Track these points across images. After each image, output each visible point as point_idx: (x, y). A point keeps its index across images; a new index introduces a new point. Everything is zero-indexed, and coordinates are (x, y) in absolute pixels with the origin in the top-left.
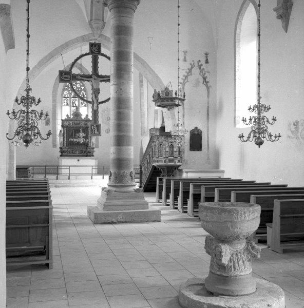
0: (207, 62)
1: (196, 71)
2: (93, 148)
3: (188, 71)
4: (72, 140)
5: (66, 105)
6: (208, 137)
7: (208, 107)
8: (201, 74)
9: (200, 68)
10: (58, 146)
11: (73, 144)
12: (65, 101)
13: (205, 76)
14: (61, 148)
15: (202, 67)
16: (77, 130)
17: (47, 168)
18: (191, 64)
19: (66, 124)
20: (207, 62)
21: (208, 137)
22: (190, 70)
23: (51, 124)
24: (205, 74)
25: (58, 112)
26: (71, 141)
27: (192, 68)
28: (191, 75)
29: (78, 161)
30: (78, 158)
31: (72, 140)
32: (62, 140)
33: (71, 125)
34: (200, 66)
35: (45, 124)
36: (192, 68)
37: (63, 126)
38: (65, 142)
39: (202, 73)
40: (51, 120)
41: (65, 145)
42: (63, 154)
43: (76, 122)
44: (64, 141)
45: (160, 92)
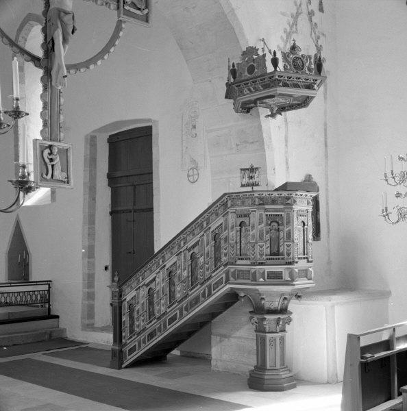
0: (321, 10)
1: (303, 22)
3: (291, 20)
6: (327, 204)
7: (325, 124)
8: (313, 35)
9: (311, 20)
13: (320, 43)
15: (314, 20)
18: (296, 5)
20: (321, 10)
21: (327, 204)
22: (296, 17)
24: (319, 38)
27: (298, 14)
28: (296, 32)
34: (311, 14)
36: (298, 14)
39: (315, 33)
45: (279, 56)
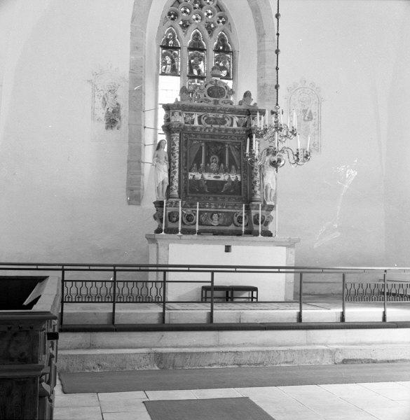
2: (271, 208)
4: (198, 176)
5: (168, 71)
10: (151, 195)
11: (202, 191)
12: (168, 60)
14: (159, 204)
16: (217, 143)
17: (120, 276)
19: (179, 119)
23: (124, 121)
25: (149, 89)
26: (196, 182)
29: (228, 249)
30: (227, 240)
31: (198, 176)
32: (164, 175)
33: (196, 123)
35: (103, 124)
37: (168, 129)
38: (176, 184)
40: (125, 111)
41: (175, 192)
42: (169, 223)
43: (211, 115)
44: (170, 177)
